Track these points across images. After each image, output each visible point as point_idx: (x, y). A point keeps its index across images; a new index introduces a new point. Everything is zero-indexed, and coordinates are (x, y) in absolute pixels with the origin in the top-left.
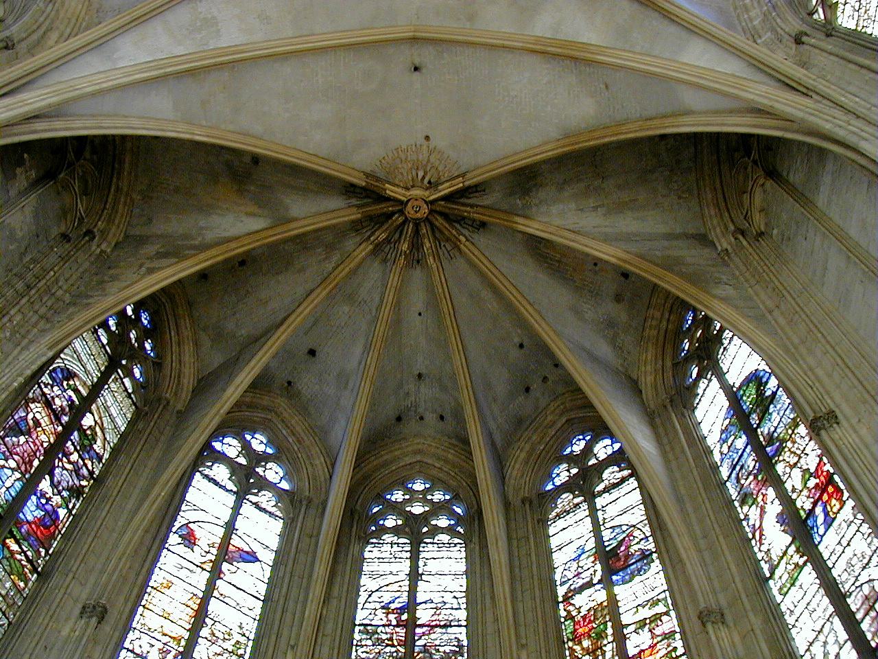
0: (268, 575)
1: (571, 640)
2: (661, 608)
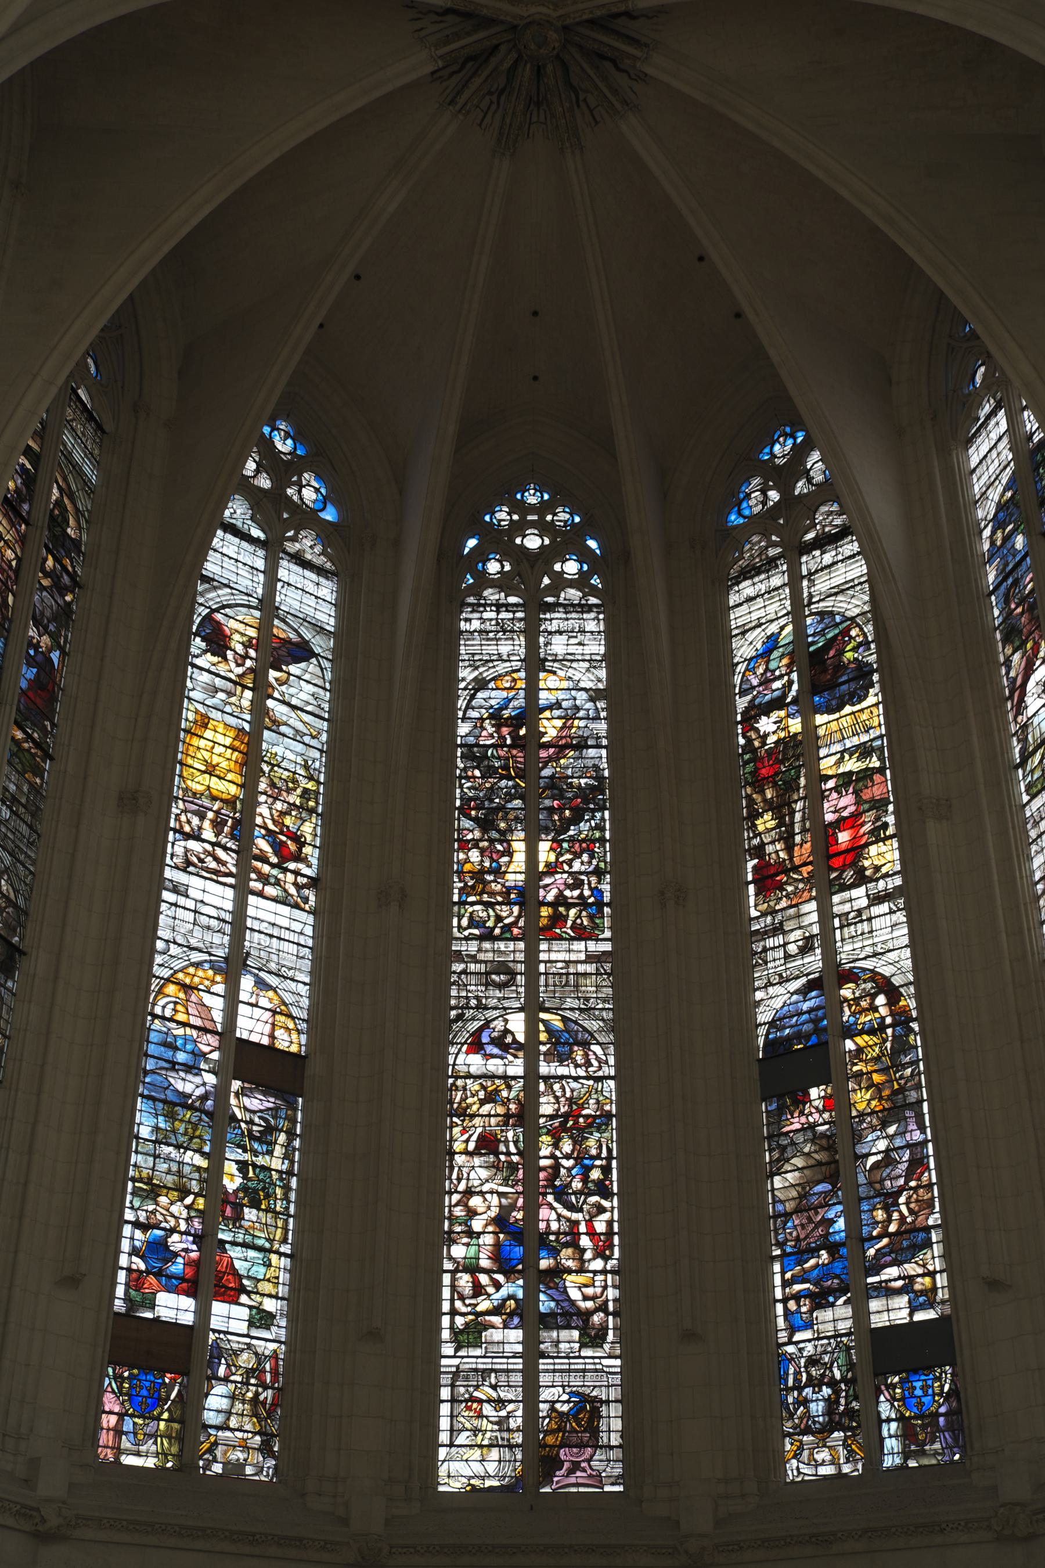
0: (328, 675)
1: (749, 784)
2: (875, 763)
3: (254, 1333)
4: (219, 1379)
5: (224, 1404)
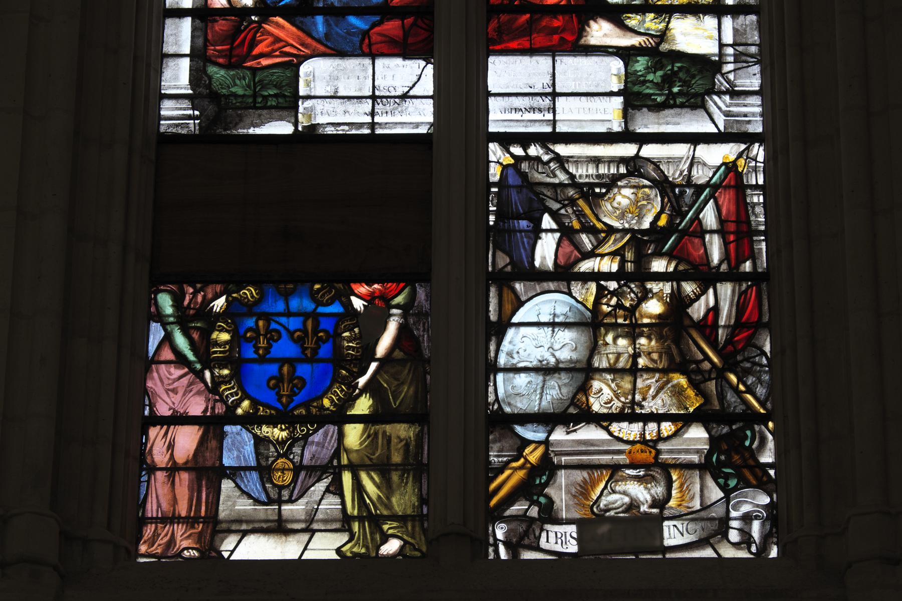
3: (647, 124)
4: (540, 276)
5: (566, 345)
